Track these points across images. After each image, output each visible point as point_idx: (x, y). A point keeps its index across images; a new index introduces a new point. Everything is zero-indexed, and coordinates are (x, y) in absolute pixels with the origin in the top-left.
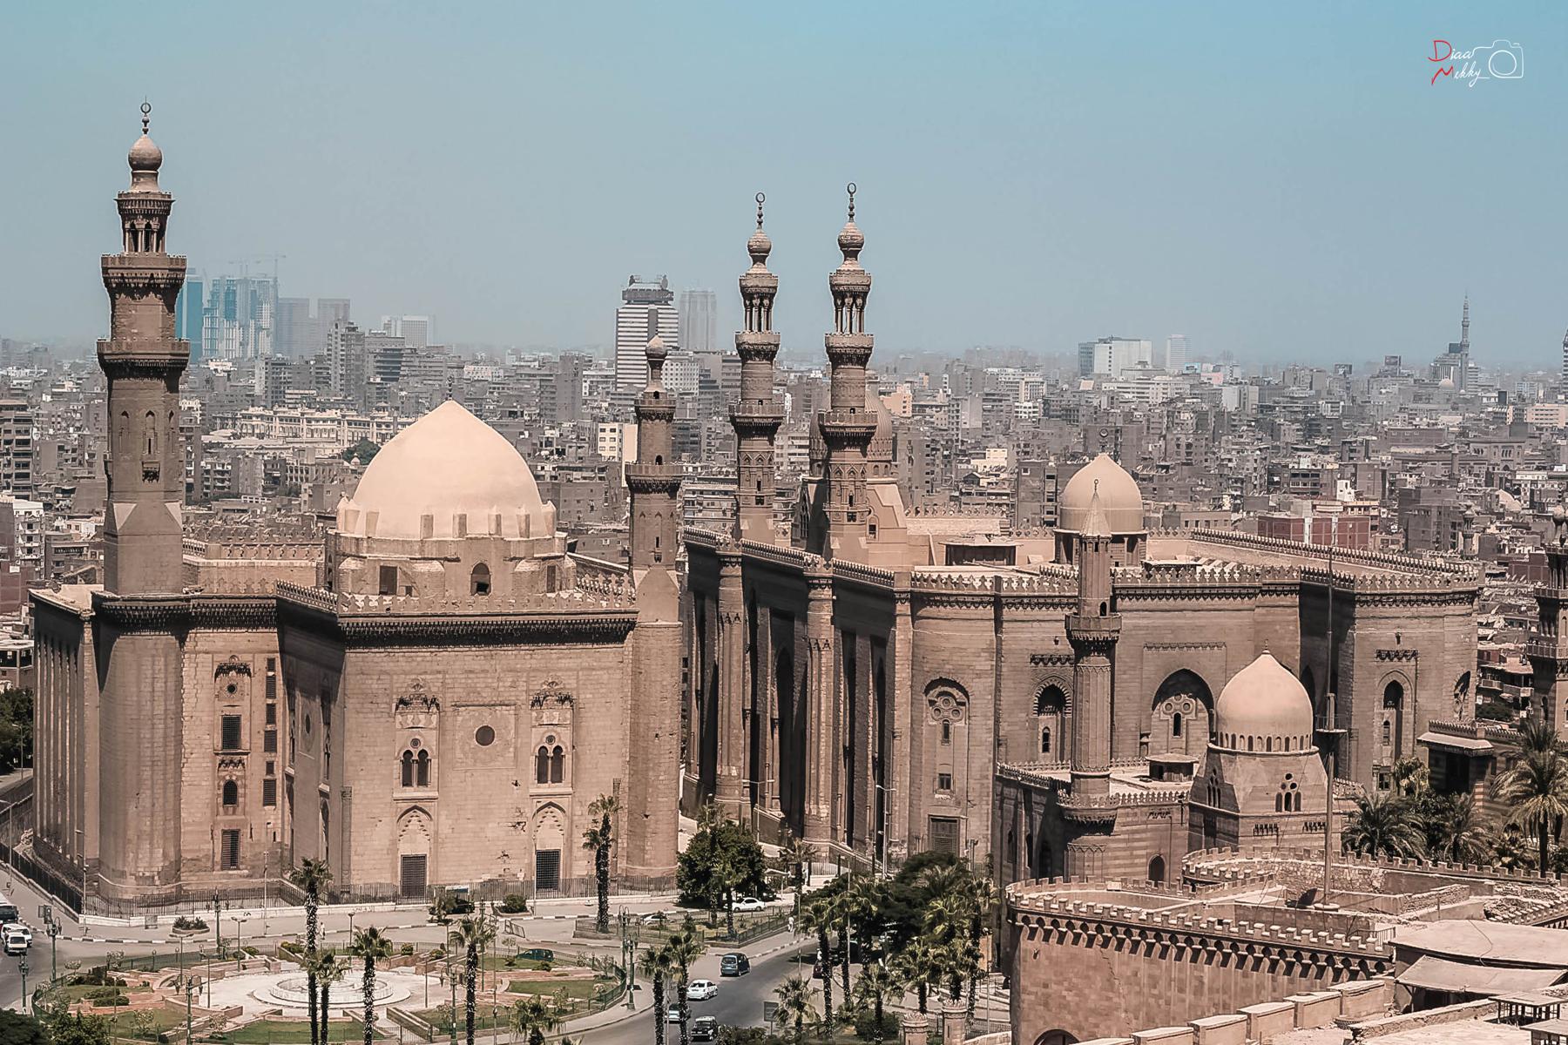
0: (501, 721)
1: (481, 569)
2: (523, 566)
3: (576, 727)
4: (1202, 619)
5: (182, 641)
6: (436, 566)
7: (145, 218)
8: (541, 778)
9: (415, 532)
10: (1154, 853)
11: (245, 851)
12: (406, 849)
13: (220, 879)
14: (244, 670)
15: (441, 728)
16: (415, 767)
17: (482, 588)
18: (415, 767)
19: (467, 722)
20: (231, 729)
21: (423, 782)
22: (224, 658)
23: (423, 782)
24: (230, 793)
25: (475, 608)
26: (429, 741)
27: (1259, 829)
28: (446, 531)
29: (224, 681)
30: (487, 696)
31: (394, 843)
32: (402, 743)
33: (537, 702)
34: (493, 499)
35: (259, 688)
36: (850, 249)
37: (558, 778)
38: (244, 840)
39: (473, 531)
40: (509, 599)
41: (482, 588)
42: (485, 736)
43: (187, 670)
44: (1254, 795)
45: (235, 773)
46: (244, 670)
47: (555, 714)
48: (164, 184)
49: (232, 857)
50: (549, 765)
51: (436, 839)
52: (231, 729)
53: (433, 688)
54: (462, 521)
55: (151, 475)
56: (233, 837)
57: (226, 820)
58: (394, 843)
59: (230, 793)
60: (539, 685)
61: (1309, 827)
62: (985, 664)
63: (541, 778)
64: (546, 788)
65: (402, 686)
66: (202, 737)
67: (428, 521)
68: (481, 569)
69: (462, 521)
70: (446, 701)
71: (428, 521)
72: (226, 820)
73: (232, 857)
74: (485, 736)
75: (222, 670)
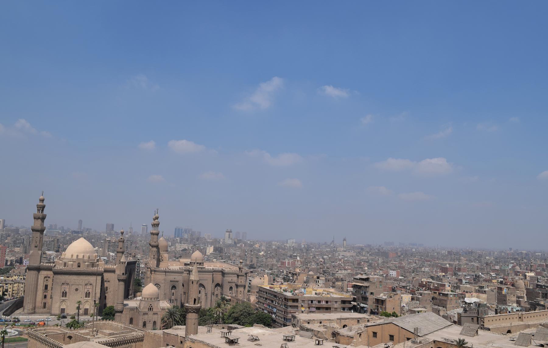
0: (81, 288)
1: (79, 263)
2: (87, 263)
3: (92, 289)
4: (204, 276)
5: (39, 273)
6: (72, 263)
7: (42, 208)
8: (86, 297)
9: (70, 257)
10: (131, 317)
11: (47, 306)
12: (62, 307)
13: (43, 310)
14: (49, 277)
15: (69, 288)
16: (64, 294)
17: (79, 266)
18: (64, 294)
19: (74, 287)
20: (46, 287)
21: (66, 296)
22: (46, 276)
23: (66, 296)
24: (45, 297)
25: (79, 269)
26: (67, 290)
27: (144, 314)
28: (75, 257)
29: (46, 279)
30: (77, 283)
31: (60, 306)
32: (63, 290)
33: (86, 285)
34: (84, 253)
35: (51, 281)
36: (157, 218)
37: (89, 297)
38: (47, 304)
39: (79, 257)
40: (83, 268)
41: (79, 266)
42: (77, 290)
43: (39, 277)
44: (143, 308)
45: (46, 294)
46: (49, 277)
47: (89, 287)
48: (45, 203)
49: (45, 307)
50: (88, 295)
51: (67, 306)
52: (46, 287)
53: (68, 281)
54: (77, 256)
55: (36, 247)
56: (45, 304)
57: (44, 301)
58: (60, 306)
59: (45, 297)
60: (86, 282)
61: (154, 314)
62: (163, 282)
63: (86, 297)
64: (86, 298)
65: (63, 281)
66: (41, 287)
67: (72, 256)
68: (79, 263)
69: (77, 256)
70: (71, 284)
71: (72, 256)
72: (44, 301)
73: (45, 307)
74: (77, 290)
75: (45, 277)
